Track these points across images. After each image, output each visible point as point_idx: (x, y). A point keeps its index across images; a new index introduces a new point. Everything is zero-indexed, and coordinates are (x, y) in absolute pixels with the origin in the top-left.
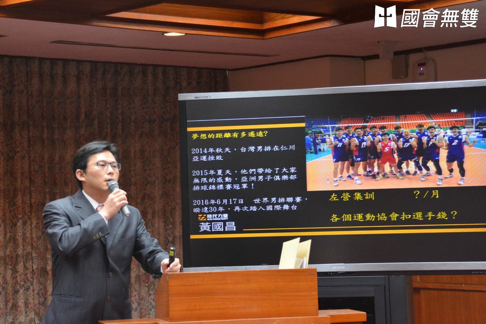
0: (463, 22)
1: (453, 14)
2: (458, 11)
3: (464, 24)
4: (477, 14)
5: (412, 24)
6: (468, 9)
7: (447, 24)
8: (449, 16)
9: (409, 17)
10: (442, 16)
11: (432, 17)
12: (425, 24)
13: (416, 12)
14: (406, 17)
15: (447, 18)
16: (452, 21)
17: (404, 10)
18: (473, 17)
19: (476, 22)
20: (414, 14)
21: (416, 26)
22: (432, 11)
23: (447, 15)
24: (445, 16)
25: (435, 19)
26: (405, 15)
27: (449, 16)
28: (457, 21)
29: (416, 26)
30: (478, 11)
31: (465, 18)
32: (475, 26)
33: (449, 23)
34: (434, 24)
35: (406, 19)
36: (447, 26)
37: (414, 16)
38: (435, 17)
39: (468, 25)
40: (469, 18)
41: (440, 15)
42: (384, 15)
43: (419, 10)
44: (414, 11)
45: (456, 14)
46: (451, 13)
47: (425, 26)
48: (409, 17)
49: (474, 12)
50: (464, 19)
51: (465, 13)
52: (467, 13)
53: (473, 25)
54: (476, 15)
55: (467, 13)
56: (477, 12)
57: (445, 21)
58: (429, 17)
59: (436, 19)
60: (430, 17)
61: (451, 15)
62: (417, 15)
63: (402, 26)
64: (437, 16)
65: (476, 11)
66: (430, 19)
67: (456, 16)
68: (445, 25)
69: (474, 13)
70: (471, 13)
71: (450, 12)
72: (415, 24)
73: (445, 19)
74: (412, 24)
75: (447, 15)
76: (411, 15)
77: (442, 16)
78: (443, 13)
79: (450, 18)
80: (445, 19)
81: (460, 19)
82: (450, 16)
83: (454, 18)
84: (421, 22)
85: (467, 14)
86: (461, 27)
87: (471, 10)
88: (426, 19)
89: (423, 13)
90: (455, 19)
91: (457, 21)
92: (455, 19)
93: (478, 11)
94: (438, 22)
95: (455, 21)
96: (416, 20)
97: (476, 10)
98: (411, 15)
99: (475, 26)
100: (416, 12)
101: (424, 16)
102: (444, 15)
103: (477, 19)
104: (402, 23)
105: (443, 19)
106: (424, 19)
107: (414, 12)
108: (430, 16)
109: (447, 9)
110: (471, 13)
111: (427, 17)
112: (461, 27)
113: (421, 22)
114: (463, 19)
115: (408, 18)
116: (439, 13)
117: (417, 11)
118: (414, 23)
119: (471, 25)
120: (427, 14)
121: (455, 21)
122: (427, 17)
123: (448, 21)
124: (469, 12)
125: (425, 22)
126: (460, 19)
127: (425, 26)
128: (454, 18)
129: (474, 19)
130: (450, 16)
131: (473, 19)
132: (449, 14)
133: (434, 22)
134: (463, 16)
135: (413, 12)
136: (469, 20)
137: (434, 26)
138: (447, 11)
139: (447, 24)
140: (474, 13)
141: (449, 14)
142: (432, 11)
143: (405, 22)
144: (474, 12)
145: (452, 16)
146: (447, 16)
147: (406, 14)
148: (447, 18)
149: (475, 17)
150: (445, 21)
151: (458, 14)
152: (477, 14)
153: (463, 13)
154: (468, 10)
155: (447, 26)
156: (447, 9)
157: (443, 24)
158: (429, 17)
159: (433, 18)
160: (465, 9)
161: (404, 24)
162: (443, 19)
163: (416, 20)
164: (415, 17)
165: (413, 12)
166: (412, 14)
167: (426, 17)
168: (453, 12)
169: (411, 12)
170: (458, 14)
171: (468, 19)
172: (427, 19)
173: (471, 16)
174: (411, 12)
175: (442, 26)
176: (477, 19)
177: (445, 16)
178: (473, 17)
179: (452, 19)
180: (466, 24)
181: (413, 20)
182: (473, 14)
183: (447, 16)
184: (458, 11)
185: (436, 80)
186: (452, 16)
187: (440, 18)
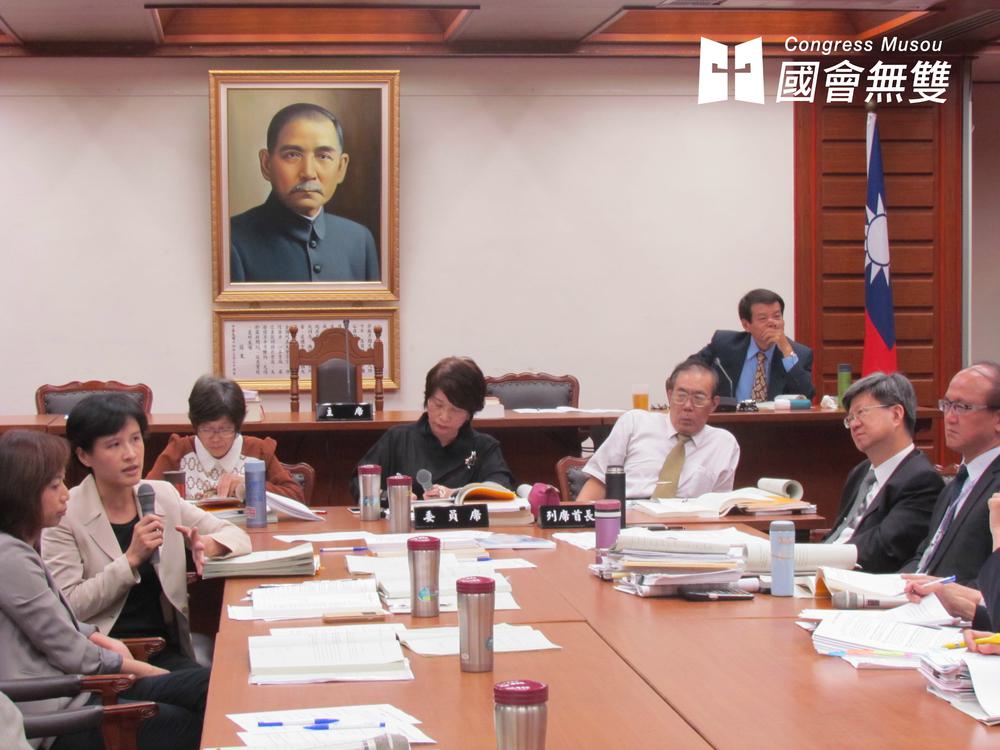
0: (915, 90)
1: (892, 73)
2: (905, 67)
3: (918, 96)
4: (948, 72)
5: (801, 95)
6: (927, 63)
7: (879, 95)
8: (884, 78)
9: (796, 79)
10: (869, 78)
11: (846, 80)
12: (830, 94)
13: (809, 68)
14: (788, 79)
15: (879, 82)
16: (890, 88)
17: (785, 64)
18: (938, 79)
19: (944, 90)
20: (807, 73)
21: (811, 100)
22: (845, 67)
23: (881, 74)
24: (876, 78)
25: (852, 84)
26: (786, 76)
27: (884, 78)
28: (903, 89)
29: (811, 100)
30: (949, 67)
31: (919, 82)
32: (942, 101)
33: (884, 94)
34: (851, 95)
35: (788, 84)
36: (879, 100)
37: (805, 76)
38: (853, 80)
39: (926, 98)
40: (930, 82)
41: (863, 76)
42: (738, 75)
43: (817, 64)
44: (806, 67)
45: (900, 73)
46: (889, 71)
47: (829, 100)
48: (796, 79)
49: (939, 70)
50: (919, 85)
51: (921, 70)
52: (925, 70)
53: (938, 97)
54: (945, 76)
55: (925, 70)
56: (946, 70)
57: (875, 88)
58: (839, 80)
59: (856, 84)
60: (842, 80)
61: (888, 74)
62: (812, 76)
63: (779, 99)
64: (857, 76)
65: (946, 65)
66: (842, 83)
67: (900, 78)
68: (875, 97)
69: (941, 69)
70: (934, 70)
71: (886, 68)
72: (809, 96)
73: (875, 84)
74: (801, 95)
75: (881, 74)
76: (798, 75)
77: (869, 78)
78: (872, 71)
79: (887, 82)
80: (875, 84)
81: (908, 84)
82: (888, 78)
83: (895, 83)
84: (822, 90)
85: (925, 73)
86: (912, 101)
87: (933, 63)
88: (832, 84)
89: (827, 70)
90: (898, 84)
91: (903, 89)
92: (898, 84)
93: (949, 67)
94: (860, 92)
95: (899, 88)
96: (810, 85)
97: (945, 63)
98: (798, 75)
99: (942, 101)
100: (809, 68)
101: (829, 76)
102: (873, 74)
103: (947, 85)
104: (779, 94)
105: (871, 83)
106: (828, 83)
107: (806, 69)
108: (843, 77)
109: (880, 62)
110: (934, 70)
111: (835, 80)
112: (912, 101)
113: (822, 90)
114: (915, 84)
115: (792, 82)
116: (861, 70)
117: (813, 68)
118: (806, 93)
119: (933, 98)
120: (834, 72)
121: (899, 88)
122: (835, 80)
123: (883, 88)
124: (928, 70)
125: (831, 90)
126: (908, 84)
127: (829, 100)
128: (895, 83)
129: (941, 84)
130: (888, 78)
131: (937, 85)
132: (885, 72)
133: (852, 90)
134: (916, 79)
135: (803, 68)
136: (930, 87)
137: (850, 100)
138: (879, 65)
139: (879, 95)
140: (941, 69)
141: (885, 72)
142: (845, 67)
143: (786, 92)
144: (939, 70)
145: (891, 78)
146: (880, 78)
147: (788, 72)
148: (879, 82)
149: (942, 79)
150: (875, 88)
151: (905, 73)
152: (948, 72)
153: (915, 70)
154: (927, 65)
155: (879, 100)
156: (880, 62)
157: (871, 95)
158: (839, 80)
159: (849, 83)
160: (920, 62)
161: (783, 95)
162: (871, 83)
163: (810, 85)
164: (809, 79)
165: (803, 68)
166: (802, 72)
167: (832, 80)
168: (893, 67)
169: (798, 68)
170: (905, 73)
171: (928, 85)
172: (836, 83)
173: (935, 78)
174: (798, 68)
175: (868, 100)
176: (947, 85)
177: (876, 78)
178: (938, 79)
179: (891, 84)
180: (923, 95)
181: (803, 86)
182: (939, 73)
183: (880, 78)
184: (905, 67)
185: (865, 141)
186: (891, 78)
187: (865, 82)
